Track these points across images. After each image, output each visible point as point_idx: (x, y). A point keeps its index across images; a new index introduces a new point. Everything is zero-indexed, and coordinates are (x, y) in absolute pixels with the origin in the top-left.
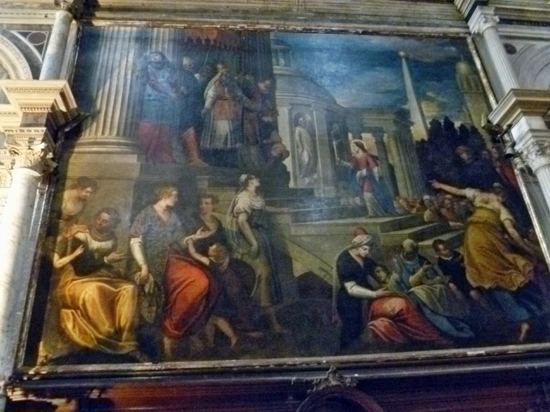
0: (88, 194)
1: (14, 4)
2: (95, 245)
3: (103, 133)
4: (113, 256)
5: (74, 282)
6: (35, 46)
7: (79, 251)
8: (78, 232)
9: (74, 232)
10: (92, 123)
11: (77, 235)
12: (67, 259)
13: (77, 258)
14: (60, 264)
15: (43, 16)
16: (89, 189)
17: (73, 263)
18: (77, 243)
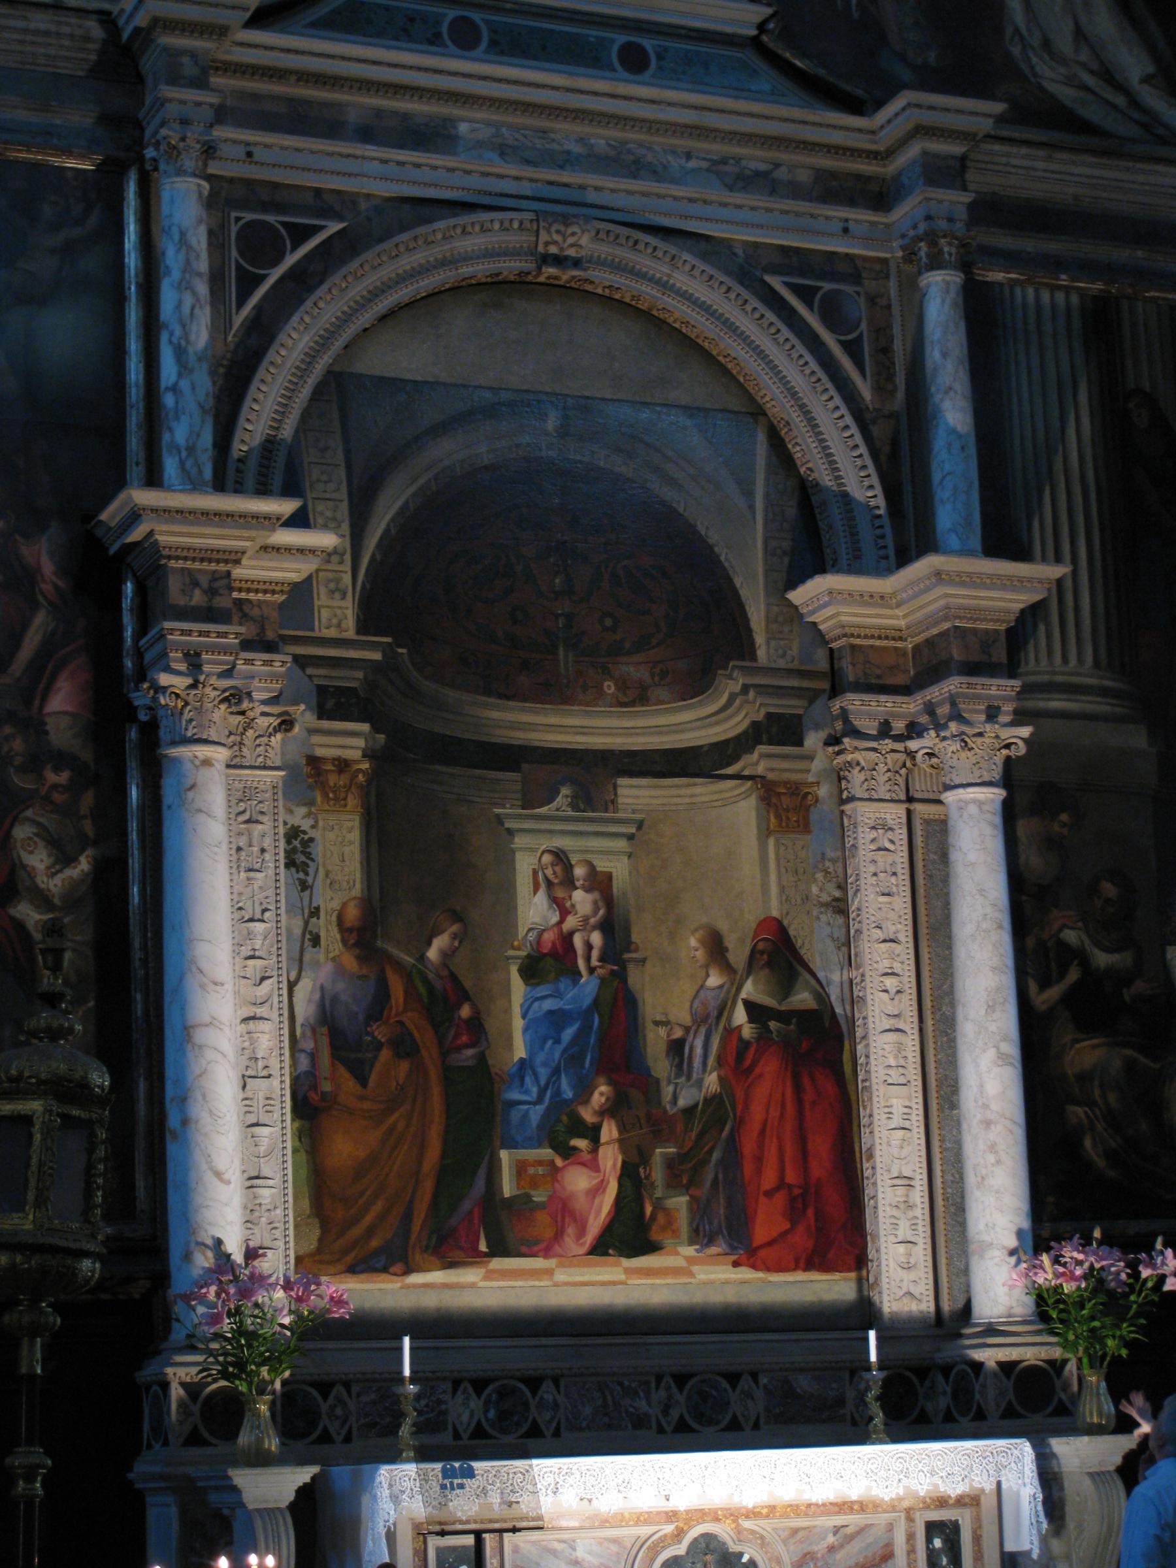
0: (1065, 831)
1: (744, 163)
2: (1101, 959)
3: (1065, 659)
4: (1139, 987)
5: (1078, 1046)
6: (840, 341)
7: (1073, 975)
8: (1064, 926)
9: (1056, 926)
10: (1035, 626)
11: (1062, 935)
12: (1054, 993)
13: (1074, 989)
14: (1043, 1003)
15: (837, 226)
16: (1064, 817)
17: (1067, 999)
18: (1068, 955)
